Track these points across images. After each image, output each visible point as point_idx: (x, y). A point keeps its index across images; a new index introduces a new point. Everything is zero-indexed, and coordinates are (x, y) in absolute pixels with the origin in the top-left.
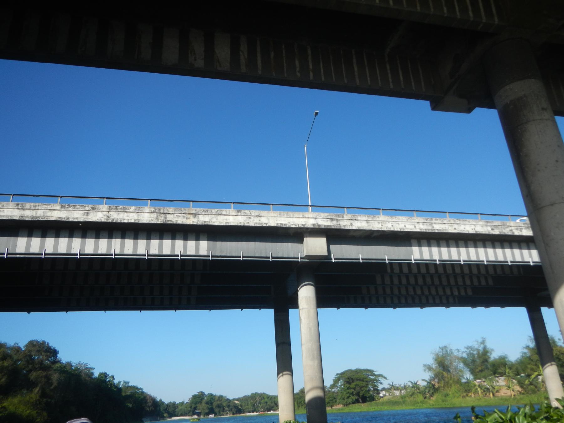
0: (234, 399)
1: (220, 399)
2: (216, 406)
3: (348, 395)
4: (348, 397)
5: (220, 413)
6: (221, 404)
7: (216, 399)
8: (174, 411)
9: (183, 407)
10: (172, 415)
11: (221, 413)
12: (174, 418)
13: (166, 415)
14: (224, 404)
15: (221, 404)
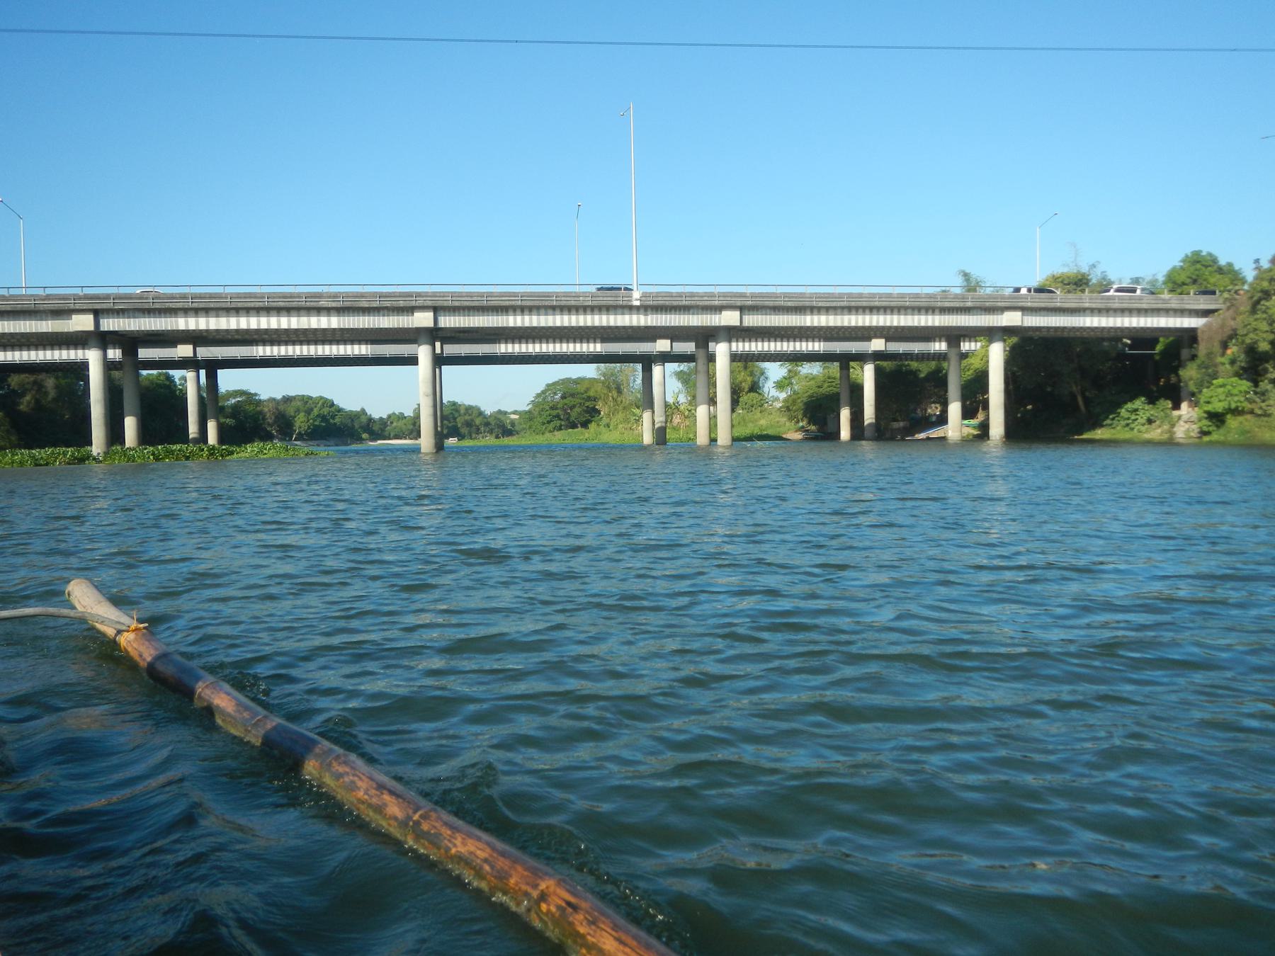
0: (515, 412)
1: (470, 412)
2: (463, 424)
3: (549, 419)
4: (549, 422)
5: (471, 436)
6: (472, 420)
7: (462, 412)
8: (383, 430)
9: (401, 424)
10: (376, 436)
11: (474, 436)
12: (379, 442)
13: (365, 436)
14: (478, 421)
15: (472, 420)
